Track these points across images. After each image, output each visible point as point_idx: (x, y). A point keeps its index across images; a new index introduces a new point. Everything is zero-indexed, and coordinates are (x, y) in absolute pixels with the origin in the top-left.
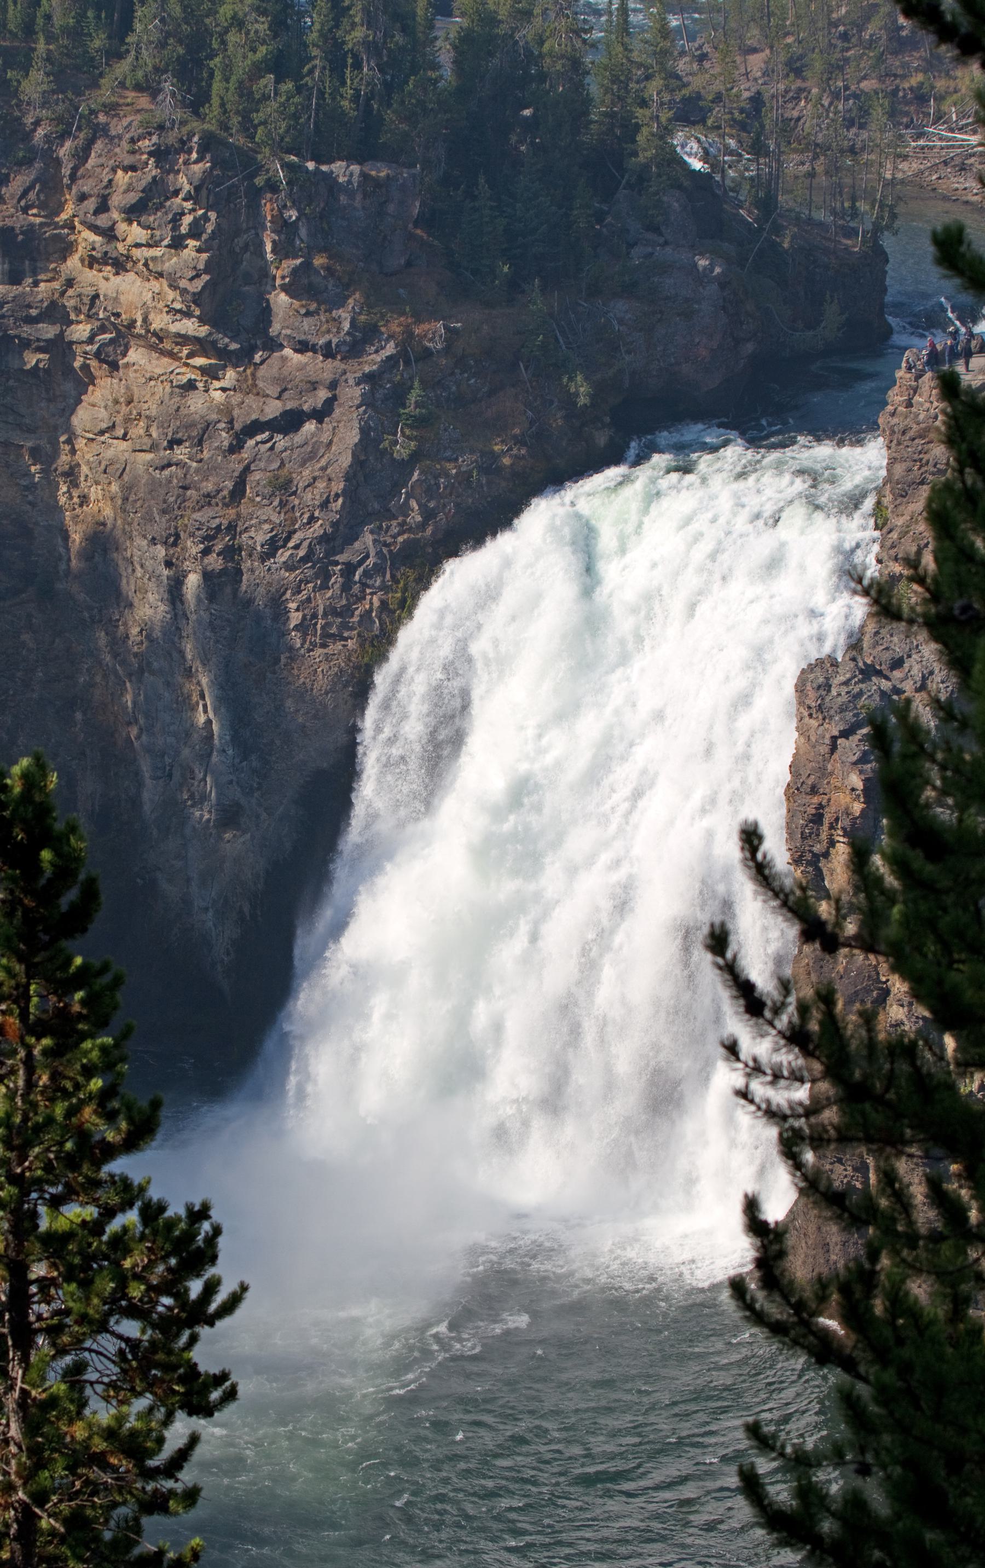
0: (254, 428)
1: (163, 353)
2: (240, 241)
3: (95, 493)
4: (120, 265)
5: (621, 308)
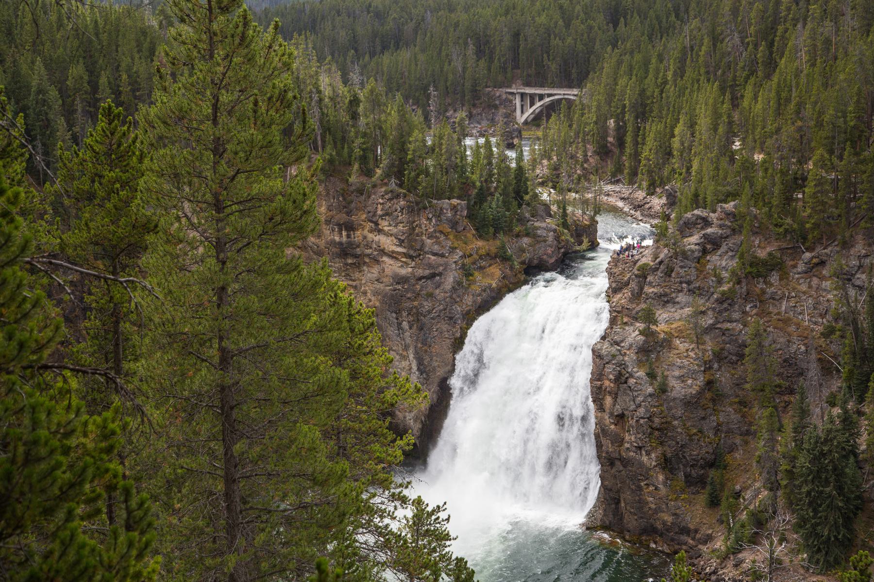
0: (420, 279)
1: (393, 257)
2: (415, 224)
3: (373, 298)
4: (380, 231)
5: (526, 241)
